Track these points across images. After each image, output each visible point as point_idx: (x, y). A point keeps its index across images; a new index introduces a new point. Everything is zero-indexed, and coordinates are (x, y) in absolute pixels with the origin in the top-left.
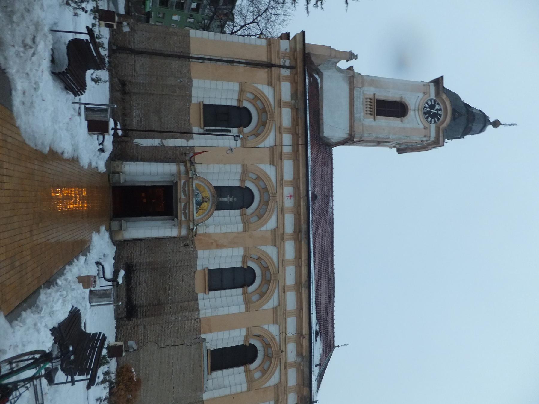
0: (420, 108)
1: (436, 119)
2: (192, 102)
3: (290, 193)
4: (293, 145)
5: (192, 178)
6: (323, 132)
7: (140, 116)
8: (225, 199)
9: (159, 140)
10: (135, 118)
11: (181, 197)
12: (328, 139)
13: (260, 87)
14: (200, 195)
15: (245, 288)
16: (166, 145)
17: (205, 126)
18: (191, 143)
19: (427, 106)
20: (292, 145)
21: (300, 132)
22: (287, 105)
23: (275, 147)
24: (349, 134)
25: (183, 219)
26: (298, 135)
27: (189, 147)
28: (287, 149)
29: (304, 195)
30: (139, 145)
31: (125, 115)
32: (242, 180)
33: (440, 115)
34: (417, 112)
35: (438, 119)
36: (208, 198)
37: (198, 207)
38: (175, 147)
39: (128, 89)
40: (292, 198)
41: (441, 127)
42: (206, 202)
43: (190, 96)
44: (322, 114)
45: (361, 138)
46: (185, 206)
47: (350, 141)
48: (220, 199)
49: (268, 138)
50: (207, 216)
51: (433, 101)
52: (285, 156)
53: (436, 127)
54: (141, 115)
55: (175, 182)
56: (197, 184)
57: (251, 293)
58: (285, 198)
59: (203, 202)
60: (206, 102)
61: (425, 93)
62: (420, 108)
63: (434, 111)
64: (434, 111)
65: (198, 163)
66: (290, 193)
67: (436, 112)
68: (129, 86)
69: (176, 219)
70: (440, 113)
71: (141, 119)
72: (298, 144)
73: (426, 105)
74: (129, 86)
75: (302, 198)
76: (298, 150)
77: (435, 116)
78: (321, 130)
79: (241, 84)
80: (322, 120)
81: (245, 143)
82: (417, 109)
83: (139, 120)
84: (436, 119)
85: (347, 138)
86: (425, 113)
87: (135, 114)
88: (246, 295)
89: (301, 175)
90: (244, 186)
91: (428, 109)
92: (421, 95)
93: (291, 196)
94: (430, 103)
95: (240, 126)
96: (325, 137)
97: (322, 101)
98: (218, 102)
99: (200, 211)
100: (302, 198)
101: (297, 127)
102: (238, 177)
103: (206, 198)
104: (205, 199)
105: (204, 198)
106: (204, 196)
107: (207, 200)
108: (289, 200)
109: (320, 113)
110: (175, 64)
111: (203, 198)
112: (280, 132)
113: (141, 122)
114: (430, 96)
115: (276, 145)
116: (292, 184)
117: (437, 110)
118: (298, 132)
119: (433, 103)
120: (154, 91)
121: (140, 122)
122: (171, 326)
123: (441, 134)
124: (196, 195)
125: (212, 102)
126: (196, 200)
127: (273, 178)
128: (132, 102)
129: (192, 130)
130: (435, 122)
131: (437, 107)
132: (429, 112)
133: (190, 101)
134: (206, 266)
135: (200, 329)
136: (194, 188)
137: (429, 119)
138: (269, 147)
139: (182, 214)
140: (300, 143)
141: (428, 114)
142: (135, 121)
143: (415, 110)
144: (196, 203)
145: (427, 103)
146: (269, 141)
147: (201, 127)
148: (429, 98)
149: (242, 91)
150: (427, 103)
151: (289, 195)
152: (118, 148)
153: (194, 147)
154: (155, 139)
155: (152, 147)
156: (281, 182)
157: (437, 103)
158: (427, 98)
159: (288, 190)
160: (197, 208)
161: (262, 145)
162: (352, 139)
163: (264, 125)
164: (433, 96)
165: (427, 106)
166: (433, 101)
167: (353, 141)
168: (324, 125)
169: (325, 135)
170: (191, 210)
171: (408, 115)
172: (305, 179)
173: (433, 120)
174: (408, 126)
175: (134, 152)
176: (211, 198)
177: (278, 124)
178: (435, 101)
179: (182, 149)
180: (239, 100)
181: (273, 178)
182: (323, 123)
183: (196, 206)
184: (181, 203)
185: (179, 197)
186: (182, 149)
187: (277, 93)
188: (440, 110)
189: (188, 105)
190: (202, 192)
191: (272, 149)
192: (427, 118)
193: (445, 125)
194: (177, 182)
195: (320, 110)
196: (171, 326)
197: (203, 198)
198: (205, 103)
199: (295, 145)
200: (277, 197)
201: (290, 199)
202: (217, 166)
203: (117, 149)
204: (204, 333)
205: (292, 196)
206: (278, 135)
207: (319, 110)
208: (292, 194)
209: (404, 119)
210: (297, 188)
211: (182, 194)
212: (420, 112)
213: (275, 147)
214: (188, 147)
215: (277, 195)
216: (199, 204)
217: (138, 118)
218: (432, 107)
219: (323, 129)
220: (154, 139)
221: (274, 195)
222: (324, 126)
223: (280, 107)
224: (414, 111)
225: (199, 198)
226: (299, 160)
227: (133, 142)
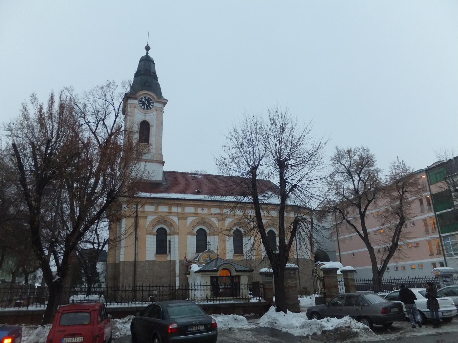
0: (145, 112)
1: (151, 102)
2: (155, 260)
4: (178, 206)
5: (200, 262)
13: (148, 223)
16: (178, 274)
17: (166, 253)
18: (177, 261)
19: (143, 107)
22: (157, 208)
23: (179, 217)
33: (148, 98)
34: (147, 115)
35: (151, 100)
38: (179, 269)
40: (203, 208)
41: (156, 100)
43: (152, 261)
49: (174, 220)
51: (140, 102)
53: (156, 103)
56: (202, 260)
59: (209, 257)
61: (135, 107)
62: (145, 112)
63: (146, 103)
64: (146, 103)
67: (147, 101)
70: (147, 98)
73: (142, 107)
76: (181, 204)
77: (149, 103)
79: (147, 234)
82: (144, 114)
84: (151, 102)
86: (147, 109)
89: (193, 203)
91: (145, 107)
92: (136, 110)
93: (203, 209)
94: (141, 105)
103: (208, 256)
106: (207, 257)
108: (204, 210)
110: (139, 269)
111: (208, 257)
114: (137, 104)
115: (178, 216)
117: (146, 100)
119: (141, 102)
123: (161, 101)
124: (207, 260)
125: (155, 249)
127: (194, 218)
130: (152, 103)
131: (143, 100)
132: (147, 106)
137: (151, 106)
138: (179, 219)
140: (177, 203)
141: (148, 108)
143: (145, 116)
145: (142, 106)
146: (175, 219)
147: (168, 256)
148: (138, 105)
149: (150, 234)
150: (142, 106)
156: (196, 214)
157: (141, 100)
158: (138, 106)
159: (200, 211)
161: (177, 224)
163: (165, 221)
164: (136, 102)
165: (143, 107)
166: (140, 102)
171: (148, 121)
173: (151, 104)
174: (155, 122)
176: (208, 253)
177: (167, 214)
178: (140, 101)
180: (154, 235)
181: (194, 218)
187: (151, 213)
188: (145, 97)
189: (156, 262)
191: (179, 218)
192: (150, 108)
193: (155, 97)
197: (208, 257)
199: (178, 205)
202: (188, 248)
206: (172, 214)
208: (201, 208)
209: (151, 124)
210: (199, 206)
212: (146, 113)
213: (179, 217)
215: (202, 217)
218: (144, 104)
219: (159, 181)
221: (202, 218)
224: (146, 117)
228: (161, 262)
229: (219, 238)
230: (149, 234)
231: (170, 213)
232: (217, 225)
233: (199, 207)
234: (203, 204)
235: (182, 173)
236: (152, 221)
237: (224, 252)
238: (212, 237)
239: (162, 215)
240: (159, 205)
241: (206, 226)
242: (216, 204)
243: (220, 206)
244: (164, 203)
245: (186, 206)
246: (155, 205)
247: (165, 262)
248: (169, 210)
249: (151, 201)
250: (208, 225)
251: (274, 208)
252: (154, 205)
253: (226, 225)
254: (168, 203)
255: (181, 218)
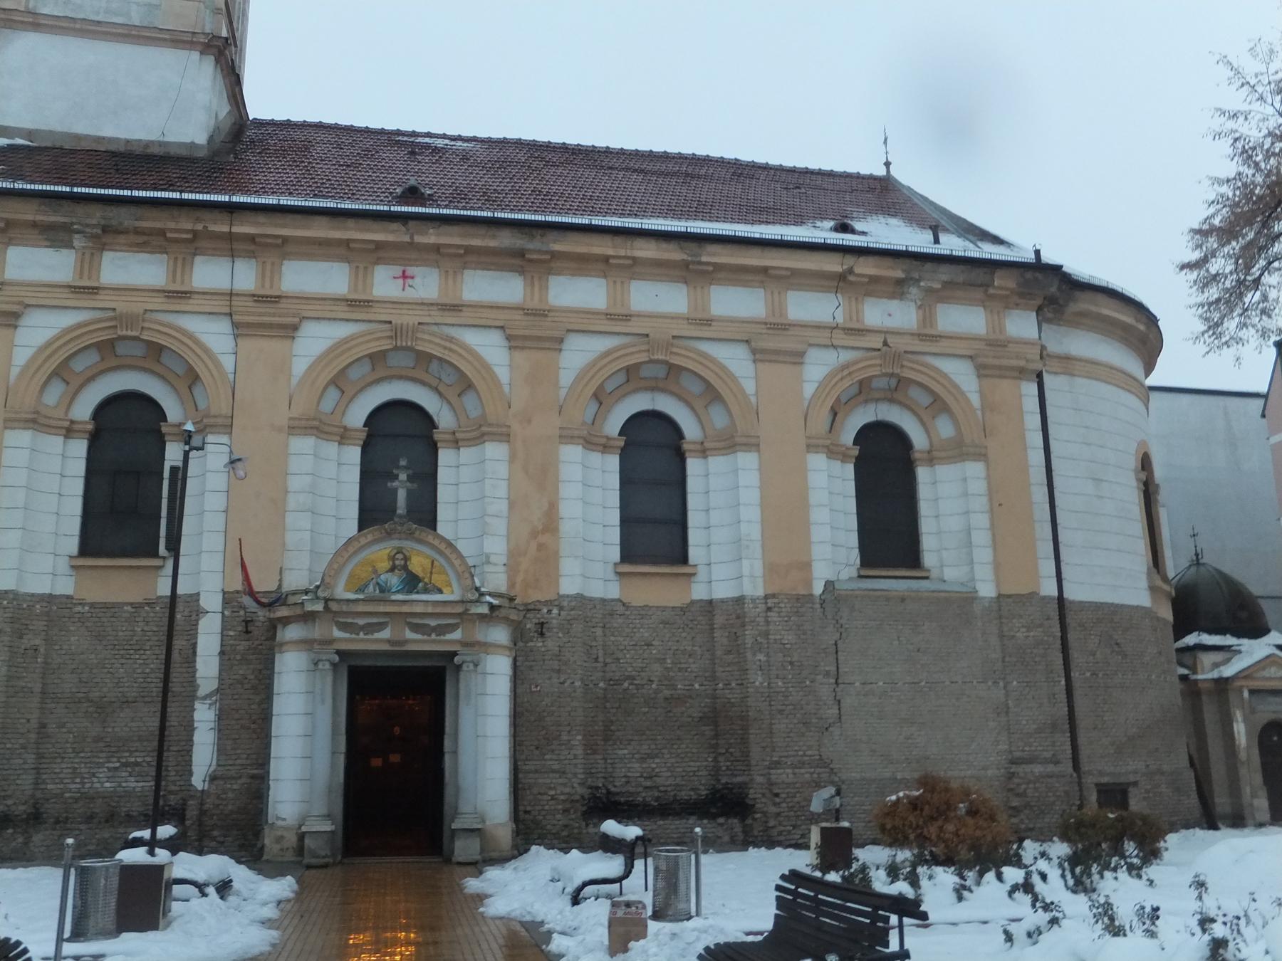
3: (395, 278)
4: (233, 254)
5: (327, 600)
6: (193, 145)
7: (116, 769)
8: (402, 495)
9: (197, 705)
10: (124, 784)
11: (389, 641)
12: (217, 129)
14: (383, 577)
15: (685, 446)
16: (214, 685)
17: (154, 554)
18: (212, 602)
20: (233, 256)
21: (189, 226)
23: (236, 318)
24: (202, 53)
25: (457, 635)
26: (196, 234)
27: (224, 608)
28: (245, 276)
29: (403, 229)
30: (215, 771)
31: (112, 816)
32: (343, 437)
36: (395, 551)
37: (420, 585)
38: (222, 653)
39: (22, 808)
40: (411, 270)
42: (406, 559)
44: (128, 141)
45: (217, 11)
46: (416, 628)
47: (227, 52)
48: (399, 511)
49: (204, 338)
50: (453, 557)
52: (267, 284)
54: (111, 765)
55: (337, 658)
57: (703, 428)
58: (410, 294)
59: (405, 567)
60: (72, 545)
65: (280, 580)
66: (395, 278)
68: (10, 802)
69: (456, 659)
71: (125, 765)
72: (231, 237)
74: (10, 802)
75: (412, 238)
78: (184, 153)
80: (148, 144)
81: (220, 421)
83: (129, 769)
85: (217, 61)
87: (107, 785)
88: (707, 445)
90: (364, 431)
93: (404, 276)
95: (160, 431)
96: (211, 139)
97: (78, 137)
98: (75, 507)
99: (437, 580)
100: (412, 238)
101: (169, 235)
102: (331, 449)
103: (393, 558)
104: (397, 563)
105: (394, 564)
106: (386, 565)
107: (399, 556)
108: (417, 281)
109: (122, 149)
111: (392, 570)
112: (185, 295)
113: (137, 764)
115: (231, 315)
116: (366, 268)
118: (187, 231)
120: (28, 721)
121: (137, 769)
122: (780, 684)
124: (382, 590)
125: (74, 526)
126: (398, 592)
127: (341, 331)
128: (67, 795)
129: (166, 596)
133: (66, 602)
134: (610, 568)
135: (798, 598)
136: (361, 596)
138: (236, 336)
139: (442, 637)
140: (225, 229)
142: (132, 784)
144: (410, 592)
147: (160, 567)
151: (401, 281)
152: (221, 839)
153: (224, 593)
154: (193, 721)
155: (219, 731)
156: (357, 304)
159: (384, 283)
160: (426, 591)
161: (228, 363)
162: (219, 43)
163: (156, 350)
167: (227, 39)
168: (166, 139)
169: (201, 138)
170: (430, 610)
172: (351, 223)
175: (235, 787)
176: (396, 543)
177: (157, 303)
179: (232, 633)
181: (341, 331)
182: (161, 144)
183: (418, 593)
184: (407, 641)
185: (386, 647)
186: (232, 633)
189: (79, 608)
190: (375, 571)
191: (240, 329)
194: (338, 652)
195: (113, 148)
196: (780, 684)
197: (392, 570)
198: (74, 549)
199: (232, 247)
200: (405, 323)
201: (412, 278)
203: (223, 842)
204: (808, 582)
205: (404, 272)
207: (114, 154)
208: (397, 270)
210: (379, 253)
211: (377, 635)
213: (236, 318)
214: (223, 613)
216: (412, 582)
217: (124, 774)
220: (196, 725)
221: (397, 332)
222: (170, 138)
223: (94, 290)
225: (394, 580)
226: (285, 240)
227: (203, 791)
228: (107, 606)
229: (512, 458)
230: (27, 421)
231: (178, 295)
232: (503, 374)
233: (379, 261)
234: (407, 239)
235: (367, 131)
236: (49, 344)
237: (541, 547)
238: (467, 454)
239: (122, 305)
240: (103, 247)
241: (434, 382)
242: (492, 243)
243: (521, 254)
244: (137, 232)
245: (285, 256)
246: (76, 243)
247: (137, 606)
248: (173, 276)
249: (39, 218)
250: (444, 377)
251: (899, 274)
252: (69, 245)
253: (566, 378)
254: (162, 233)
255: (249, 325)
